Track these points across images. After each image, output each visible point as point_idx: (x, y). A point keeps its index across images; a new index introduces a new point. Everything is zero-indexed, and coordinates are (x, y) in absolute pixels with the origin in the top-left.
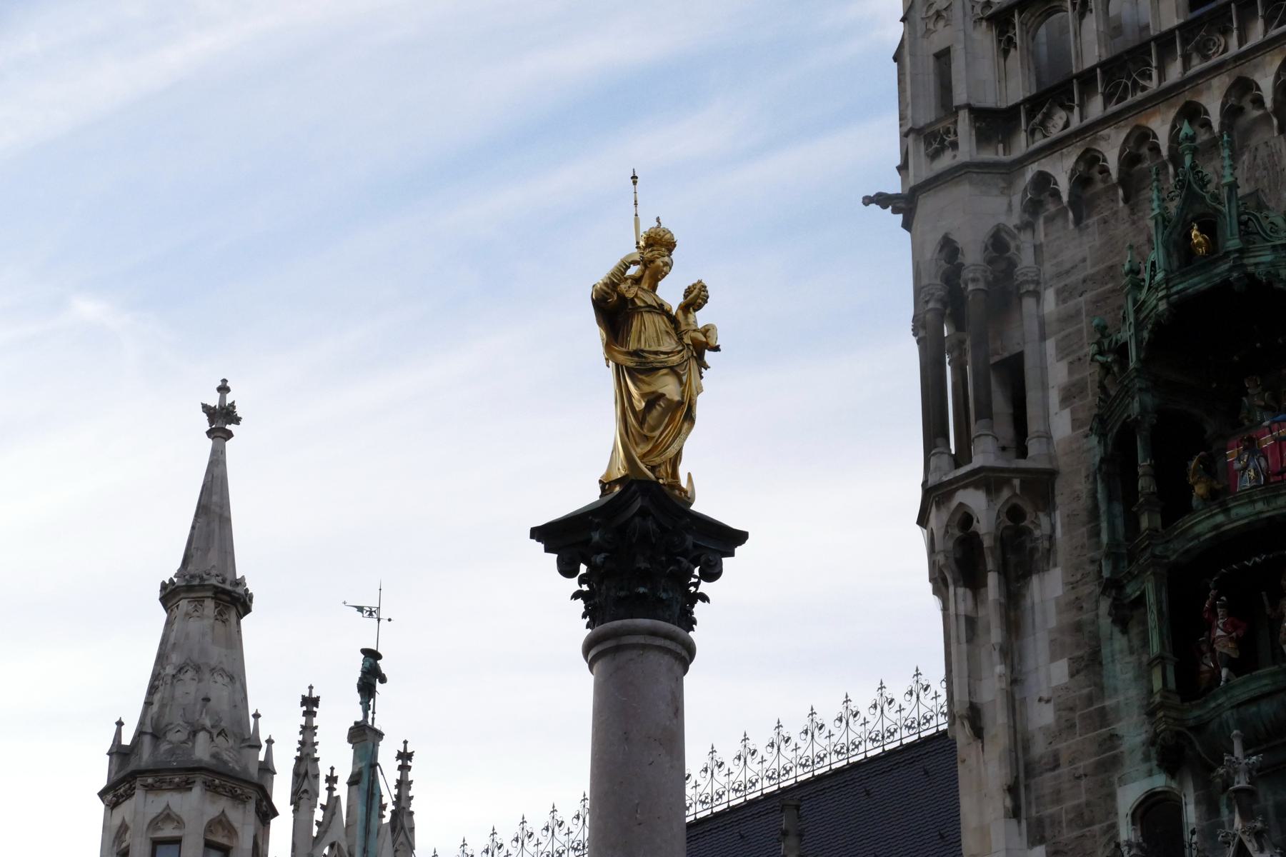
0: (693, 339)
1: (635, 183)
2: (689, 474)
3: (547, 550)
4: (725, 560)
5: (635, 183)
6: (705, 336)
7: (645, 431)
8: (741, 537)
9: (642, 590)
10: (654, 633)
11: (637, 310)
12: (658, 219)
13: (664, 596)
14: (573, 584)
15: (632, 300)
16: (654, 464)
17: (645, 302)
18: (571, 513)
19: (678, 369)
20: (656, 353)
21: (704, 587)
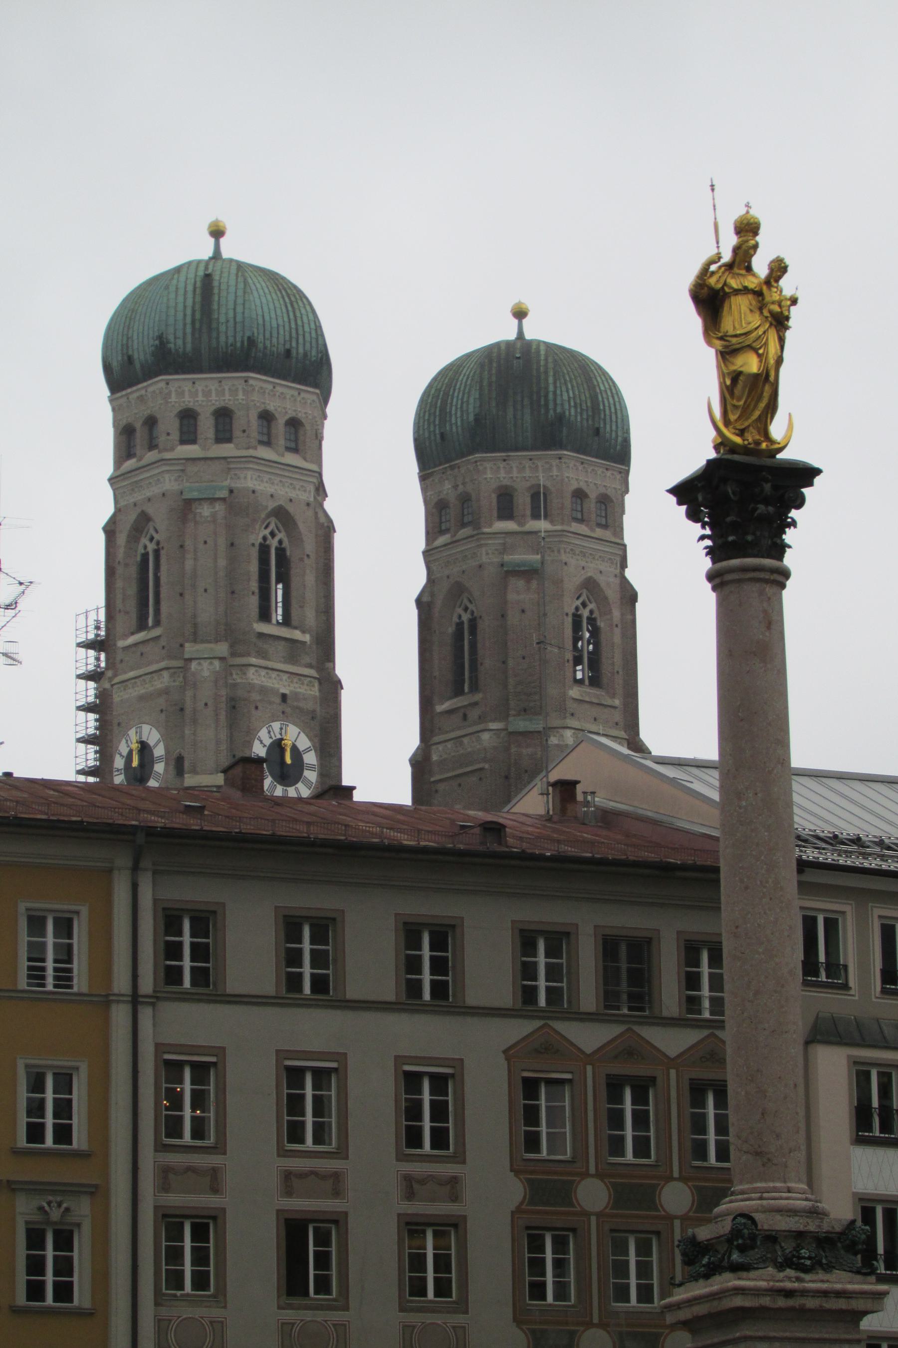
0: (770, 312)
1: (713, 190)
2: (790, 414)
3: (680, 503)
4: (805, 491)
5: (713, 190)
6: (780, 306)
7: (735, 402)
8: (817, 472)
9: (731, 538)
10: (744, 569)
11: (726, 296)
12: (748, 206)
13: (750, 538)
14: (696, 529)
15: (722, 288)
16: (743, 427)
17: (731, 288)
18: (692, 475)
19: (754, 345)
20: (736, 336)
21: (794, 513)
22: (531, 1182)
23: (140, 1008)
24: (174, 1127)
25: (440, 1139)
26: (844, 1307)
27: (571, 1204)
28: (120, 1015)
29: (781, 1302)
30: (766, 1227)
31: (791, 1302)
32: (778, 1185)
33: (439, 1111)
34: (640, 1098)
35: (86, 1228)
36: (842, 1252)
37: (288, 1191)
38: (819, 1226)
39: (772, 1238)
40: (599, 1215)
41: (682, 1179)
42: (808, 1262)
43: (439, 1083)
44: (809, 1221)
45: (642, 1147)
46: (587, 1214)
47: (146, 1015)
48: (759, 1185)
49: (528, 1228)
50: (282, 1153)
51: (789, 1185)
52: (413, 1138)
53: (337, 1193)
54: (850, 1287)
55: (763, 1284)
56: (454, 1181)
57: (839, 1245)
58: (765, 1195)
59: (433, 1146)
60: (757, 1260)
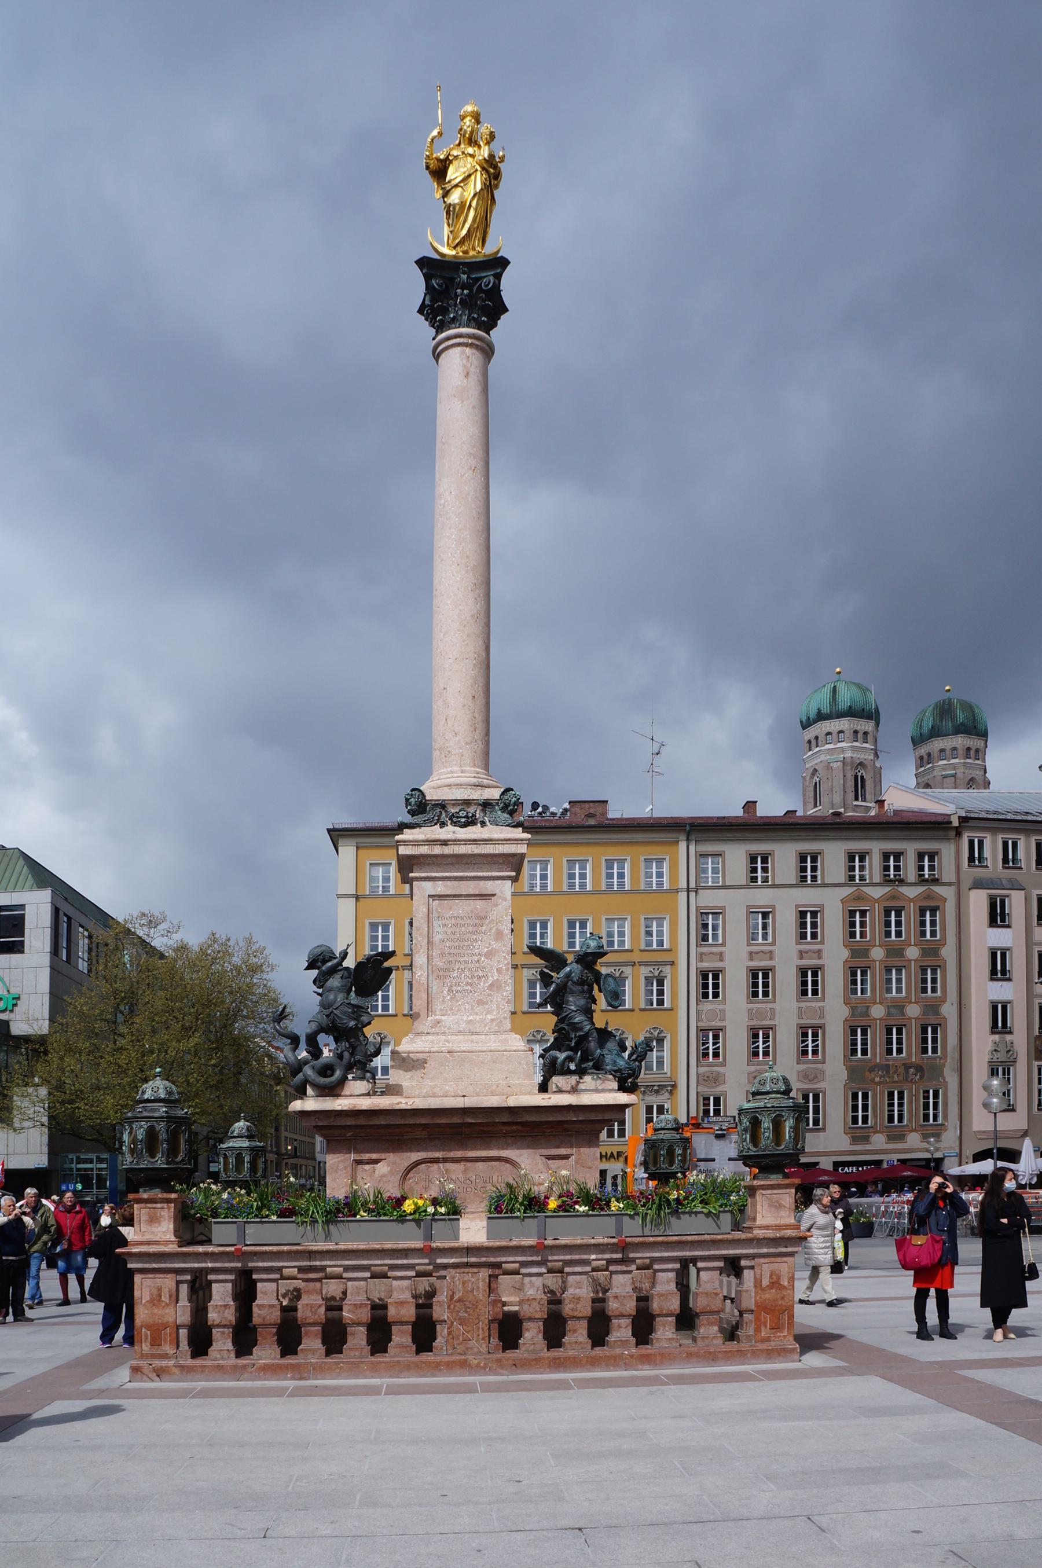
22: (851, 950)
23: (690, 893)
24: (705, 938)
25: (814, 935)
26: (492, 852)
27: (868, 958)
28: (683, 896)
29: (437, 850)
30: (435, 798)
31: (446, 850)
32: (455, 769)
33: (814, 925)
34: (898, 914)
35: (669, 977)
36: (499, 812)
37: (752, 960)
38: (481, 795)
39: (442, 805)
40: (879, 961)
41: (915, 945)
42: (463, 820)
43: (814, 914)
44: (473, 792)
45: (899, 934)
46: (876, 961)
47: (692, 895)
48: (442, 771)
49: (850, 968)
50: (749, 944)
51: (463, 769)
52: (803, 936)
53: (771, 959)
54: (496, 836)
55: (422, 837)
56: (820, 951)
57: (497, 807)
58: (441, 777)
59: (812, 938)
60: (424, 821)
